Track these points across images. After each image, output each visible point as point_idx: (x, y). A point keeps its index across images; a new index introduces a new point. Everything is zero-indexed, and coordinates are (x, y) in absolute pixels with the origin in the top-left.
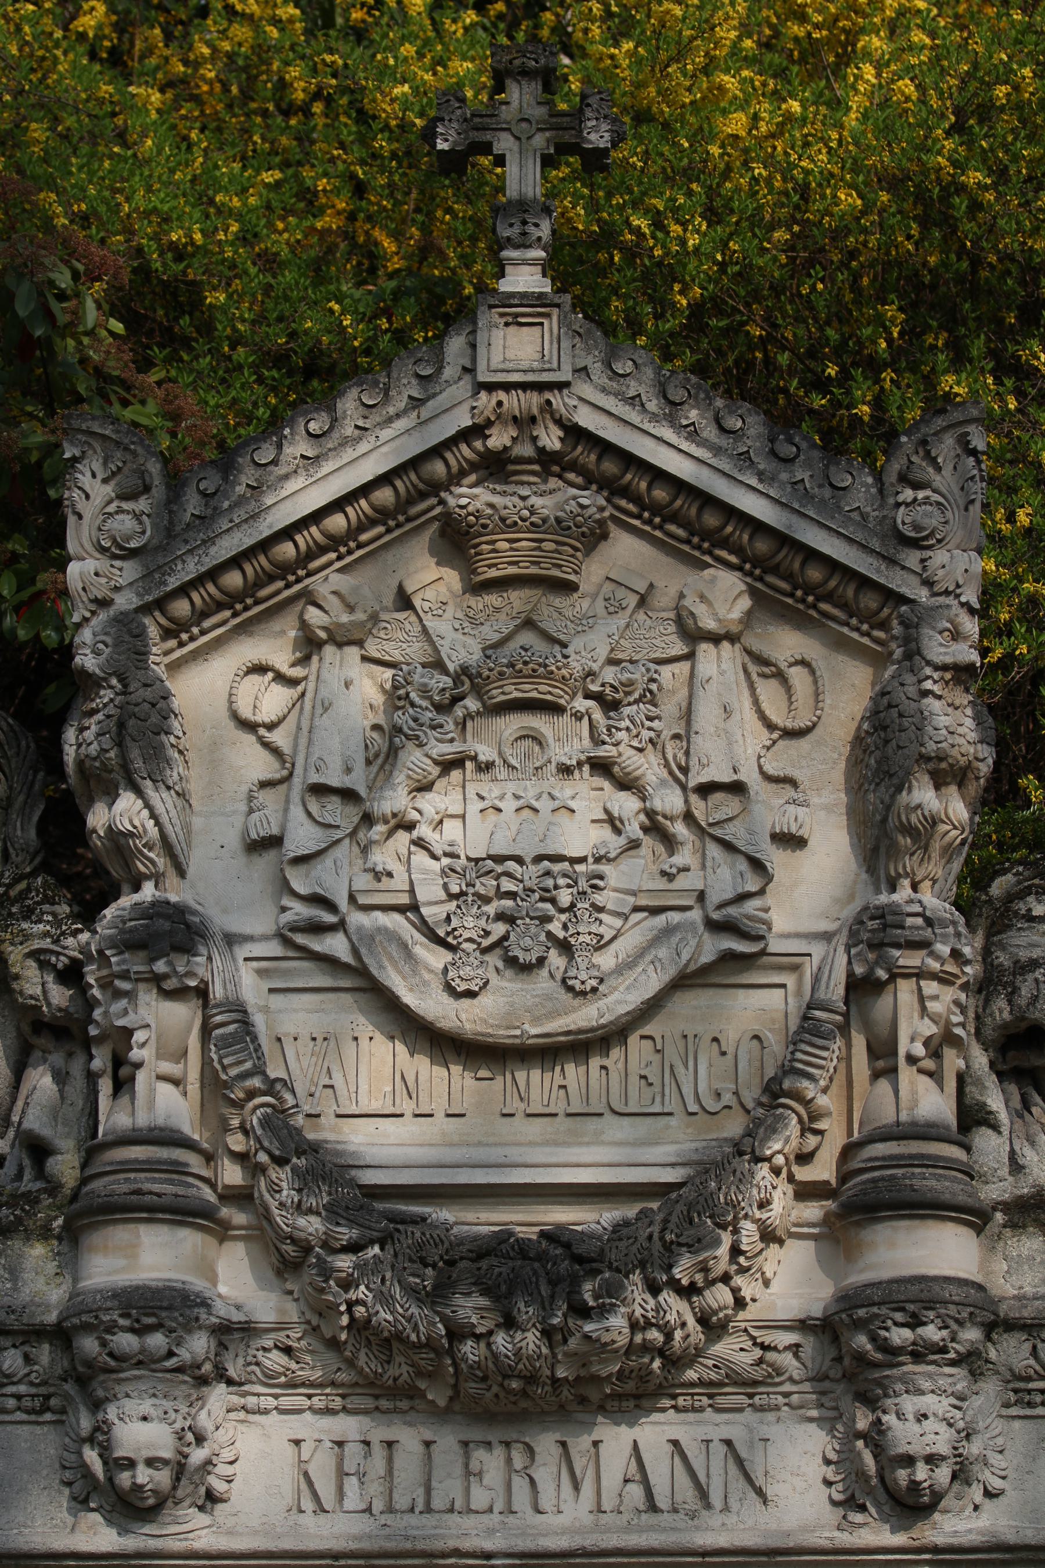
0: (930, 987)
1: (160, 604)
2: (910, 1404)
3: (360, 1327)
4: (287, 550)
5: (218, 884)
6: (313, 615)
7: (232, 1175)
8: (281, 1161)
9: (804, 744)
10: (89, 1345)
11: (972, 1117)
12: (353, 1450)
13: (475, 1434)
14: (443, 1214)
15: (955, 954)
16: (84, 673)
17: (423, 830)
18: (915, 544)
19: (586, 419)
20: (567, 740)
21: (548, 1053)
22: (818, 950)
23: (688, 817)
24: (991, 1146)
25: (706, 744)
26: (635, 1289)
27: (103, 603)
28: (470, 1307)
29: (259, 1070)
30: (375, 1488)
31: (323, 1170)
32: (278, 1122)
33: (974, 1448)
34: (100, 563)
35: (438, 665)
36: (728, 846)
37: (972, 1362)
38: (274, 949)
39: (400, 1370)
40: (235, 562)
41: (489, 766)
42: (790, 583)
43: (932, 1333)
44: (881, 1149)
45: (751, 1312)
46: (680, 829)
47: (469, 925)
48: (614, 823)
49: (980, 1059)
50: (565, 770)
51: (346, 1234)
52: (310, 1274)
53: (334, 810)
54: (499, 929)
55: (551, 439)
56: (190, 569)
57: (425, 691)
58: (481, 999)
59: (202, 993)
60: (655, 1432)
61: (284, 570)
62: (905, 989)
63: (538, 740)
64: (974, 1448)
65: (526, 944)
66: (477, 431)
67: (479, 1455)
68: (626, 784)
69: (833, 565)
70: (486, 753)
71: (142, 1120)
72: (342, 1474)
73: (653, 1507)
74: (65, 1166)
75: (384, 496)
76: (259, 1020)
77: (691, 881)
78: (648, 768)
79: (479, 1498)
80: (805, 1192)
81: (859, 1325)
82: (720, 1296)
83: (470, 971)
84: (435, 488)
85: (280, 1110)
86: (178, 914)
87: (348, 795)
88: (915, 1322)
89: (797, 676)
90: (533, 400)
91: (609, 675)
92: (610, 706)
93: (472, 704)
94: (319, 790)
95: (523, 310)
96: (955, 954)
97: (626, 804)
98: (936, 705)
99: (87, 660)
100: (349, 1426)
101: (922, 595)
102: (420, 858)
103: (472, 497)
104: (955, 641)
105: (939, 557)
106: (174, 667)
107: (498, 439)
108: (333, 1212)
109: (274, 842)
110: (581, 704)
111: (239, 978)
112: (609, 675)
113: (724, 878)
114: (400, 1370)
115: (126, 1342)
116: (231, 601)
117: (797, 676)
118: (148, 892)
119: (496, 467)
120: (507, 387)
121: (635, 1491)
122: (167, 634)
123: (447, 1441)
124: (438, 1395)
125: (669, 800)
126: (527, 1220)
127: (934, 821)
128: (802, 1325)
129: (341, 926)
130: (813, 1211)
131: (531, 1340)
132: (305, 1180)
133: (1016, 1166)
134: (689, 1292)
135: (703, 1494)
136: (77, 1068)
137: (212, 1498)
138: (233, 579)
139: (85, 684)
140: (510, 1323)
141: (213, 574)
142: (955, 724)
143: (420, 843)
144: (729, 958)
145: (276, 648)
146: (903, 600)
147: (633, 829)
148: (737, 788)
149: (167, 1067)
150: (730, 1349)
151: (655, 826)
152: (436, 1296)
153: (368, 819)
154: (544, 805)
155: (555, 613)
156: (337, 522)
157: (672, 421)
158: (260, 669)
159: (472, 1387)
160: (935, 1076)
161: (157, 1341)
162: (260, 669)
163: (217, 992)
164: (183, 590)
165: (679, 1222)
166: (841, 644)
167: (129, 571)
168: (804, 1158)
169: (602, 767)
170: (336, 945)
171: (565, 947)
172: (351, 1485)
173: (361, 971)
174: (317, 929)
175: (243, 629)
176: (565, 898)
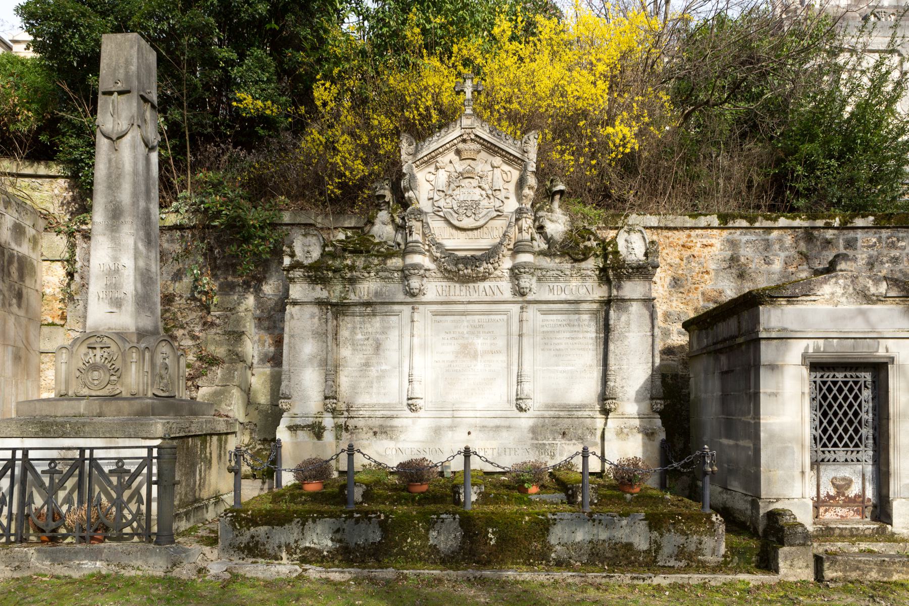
3: (445, 269)
4: (433, 154)
5: (424, 205)
10: (407, 272)
11: (532, 239)
19: (478, 133)
20: (474, 183)
21: (472, 230)
28: (461, 266)
31: (439, 246)
37: (532, 274)
48: (482, 195)
49: (534, 230)
53: (442, 194)
55: (473, 137)
56: (420, 157)
60: (486, 284)
61: (433, 157)
74: (403, 247)
77: (493, 204)
78: (487, 187)
80: (509, 250)
82: (496, 265)
90: (470, 131)
92: (481, 178)
97: (484, 193)
99: (404, 171)
100: (444, 284)
103: (461, 146)
104: (532, 167)
107: (465, 137)
108: (441, 252)
113: (498, 203)
116: (425, 162)
118: (413, 206)
119: (464, 141)
123: (457, 285)
125: (490, 192)
126: (469, 254)
130: (510, 252)
131: (470, 271)
132: (437, 248)
139: (405, 174)
142: (532, 181)
144: (499, 216)
145: (432, 169)
150: (498, 273)
152: (456, 265)
165: (491, 254)
166: (515, 168)
167: (411, 157)
169: (480, 187)
170: (441, 214)
173: (445, 218)
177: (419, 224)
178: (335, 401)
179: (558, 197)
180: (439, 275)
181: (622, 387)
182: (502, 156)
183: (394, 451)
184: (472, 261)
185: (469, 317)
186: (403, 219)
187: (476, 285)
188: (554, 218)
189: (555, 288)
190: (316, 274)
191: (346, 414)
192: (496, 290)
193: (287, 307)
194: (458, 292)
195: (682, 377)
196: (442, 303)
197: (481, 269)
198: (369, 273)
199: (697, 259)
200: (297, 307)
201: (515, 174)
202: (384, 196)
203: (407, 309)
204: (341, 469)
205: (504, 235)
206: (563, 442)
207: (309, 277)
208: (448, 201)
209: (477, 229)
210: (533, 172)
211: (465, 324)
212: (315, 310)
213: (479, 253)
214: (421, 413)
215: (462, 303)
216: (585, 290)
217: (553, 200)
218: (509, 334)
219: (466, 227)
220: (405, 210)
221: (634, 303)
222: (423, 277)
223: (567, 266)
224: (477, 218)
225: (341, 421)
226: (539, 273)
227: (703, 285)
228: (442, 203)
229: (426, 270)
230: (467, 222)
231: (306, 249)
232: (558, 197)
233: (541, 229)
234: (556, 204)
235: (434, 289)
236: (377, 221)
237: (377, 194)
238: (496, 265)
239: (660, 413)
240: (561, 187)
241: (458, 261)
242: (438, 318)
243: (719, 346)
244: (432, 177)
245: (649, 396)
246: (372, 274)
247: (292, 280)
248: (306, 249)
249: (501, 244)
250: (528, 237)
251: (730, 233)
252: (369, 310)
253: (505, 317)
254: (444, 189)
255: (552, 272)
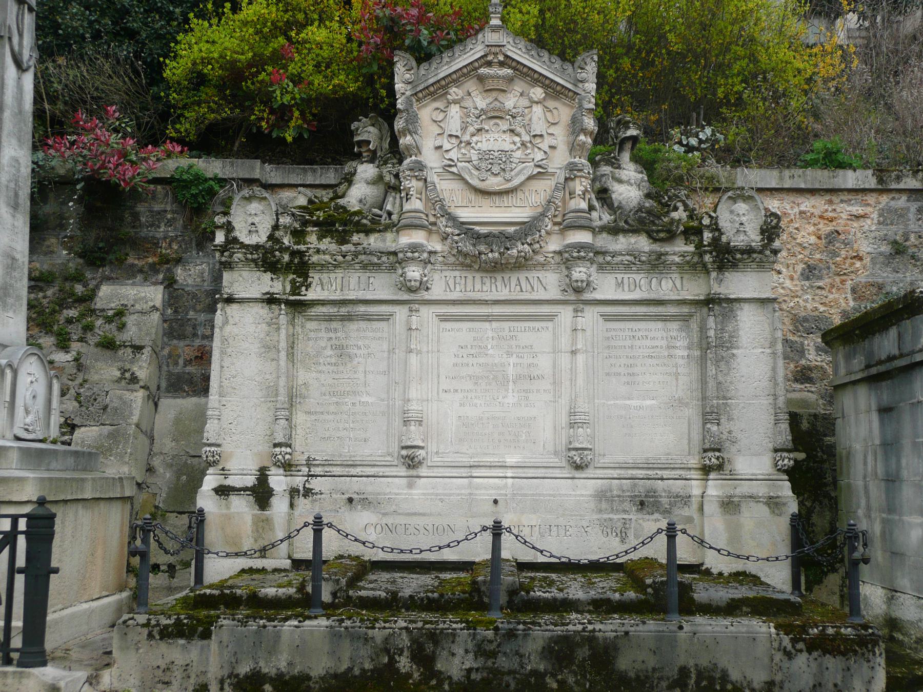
0: (583, 180)
1: (416, 94)
2: (578, 269)
3: (460, 252)
4: (443, 83)
6: (449, 97)
7: (432, 219)
8: (443, 216)
9: (556, 127)
10: (401, 255)
11: (591, 208)
12: (458, 280)
13: (484, 275)
14: (477, 228)
15: (589, 173)
16: (399, 109)
17: (473, 145)
18: (581, 82)
19: (509, 53)
20: (504, 126)
22: (558, 171)
23: (531, 142)
24: (595, 215)
25: (533, 126)
26: (519, 244)
27: (403, 94)
29: (438, 196)
30: (463, 286)
31: (452, 218)
32: (442, 207)
33: (591, 279)
34: (403, 85)
35: (476, 108)
36: (539, 148)
38: (441, 170)
39: (468, 261)
40: (432, 85)
41: (487, 131)
42: (554, 91)
43: (582, 254)
44: (572, 214)
45: (543, 249)
46: (529, 145)
47: (483, 165)
48: (514, 143)
49: (593, 196)
50: (504, 132)
51: (457, 232)
52: (449, 240)
53: (454, 140)
54: (490, 166)
55: (501, 58)
57: (474, 114)
58: (487, 182)
59: (425, 180)
61: (442, 87)
62: (577, 181)
63: (498, 125)
64: (591, 279)
65: (496, 169)
66: (486, 56)
67: (485, 279)
68: (518, 135)
69: (563, 86)
70: (487, 127)
71: (413, 207)
72: (455, 283)
73: (522, 291)
74: (395, 217)
75: (465, 71)
76: (438, 186)
77: (531, 156)
79: (485, 289)
80: (555, 224)
81: (566, 252)
82: (537, 246)
83: (484, 175)
84: (476, 69)
85: (443, 205)
86: (419, 162)
87: (457, 137)
88: (579, 252)
89: (555, 111)
90: (498, 49)
91: (514, 111)
93: (484, 117)
94: (450, 136)
95: (495, 29)
96: (589, 173)
97: (517, 139)
98: (585, 118)
99: (399, 106)
100: (457, 273)
101: (583, 93)
102: (472, 151)
105: (586, 85)
106: (418, 109)
107: (490, 58)
109: (440, 147)
110: (508, 117)
111: (433, 177)
112: (514, 111)
113: (539, 156)
114: (468, 261)
115: (409, 255)
116: (431, 94)
117: (555, 111)
118: (414, 158)
119: (489, 64)
120: (492, 46)
121: (518, 287)
122: (417, 101)
123: (478, 276)
124: (477, 267)
125: (526, 138)
127: (584, 143)
128: (554, 252)
129: (456, 165)
130: (557, 228)
131: (496, 255)
132: (448, 219)
133: (600, 219)
134: (530, 245)
135: (533, 288)
136: (398, 196)
137: (428, 288)
138: (432, 89)
140: (492, 251)
141: (427, 88)
143: (473, 147)
144: (539, 173)
145: (439, 104)
146: (578, 94)
147: (519, 145)
148: (541, 136)
149: (419, 196)
151: (523, 144)
153: (461, 142)
154: (500, 139)
155: (501, 97)
156: (454, 76)
157: (528, 54)
158: (437, 109)
159: (483, 265)
160: (584, 199)
161: (416, 254)
162: (437, 109)
163: (429, 180)
164: (421, 91)
165: (528, 229)
166: (564, 104)
167: (409, 87)
168: (555, 216)
169: (512, 131)
170: (454, 169)
171: (504, 170)
172: (457, 286)
173: (460, 175)
174: (450, 166)
175: (435, 100)
176: (504, 159)
177: (421, 184)
178: (288, 450)
179: (628, 145)
180: (452, 260)
181: (730, 432)
182: (545, 87)
183: (379, 527)
184: (500, 238)
185: (494, 325)
186: (397, 176)
187: (506, 276)
188: (624, 178)
189: (626, 281)
190: (267, 259)
191: (305, 470)
192: (536, 283)
193: (219, 306)
194: (478, 286)
195: (826, 418)
196: (454, 302)
197: (514, 252)
198: (344, 257)
199: (842, 237)
200: (235, 306)
201: (564, 113)
202: (368, 142)
203: (401, 313)
204: (297, 556)
205: (549, 202)
206: (640, 516)
207: (253, 260)
208: (463, 151)
209: (507, 192)
210: (590, 110)
211: (490, 334)
212: (262, 311)
213: (512, 229)
214: (423, 471)
215: (485, 302)
216: (670, 284)
217: (621, 150)
218: (555, 351)
219: (491, 189)
220: (400, 162)
221: (746, 307)
222: (427, 262)
223: (642, 243)
224: (507, 176)
225: (298, 481)
226: (600, 259)
227: (853, 276)
228: (453, 155)
229: (430, 253)
230: (494, 183)
231: (252, 221)
232: (628, 145)
233: (603, 194)
234: (626, 156)
235: (444, 284)
236: (357, 178)
237: (356, 139)
238: (537, 246)
239: (787, 472)
240: (632, 132)
241: (478, 238)
242: (448, 325)
243: (874, 371)
244: (440, 117)
245: (771, 446)
246: (349, 258)
247: (228, 266)
248: (250, 220)
249: (543, 215)
250: (584, 205)
251: (893, 199)
252: (344, 310)
253: (550, 324)
254: (459, 134)
255: (620, 258)
